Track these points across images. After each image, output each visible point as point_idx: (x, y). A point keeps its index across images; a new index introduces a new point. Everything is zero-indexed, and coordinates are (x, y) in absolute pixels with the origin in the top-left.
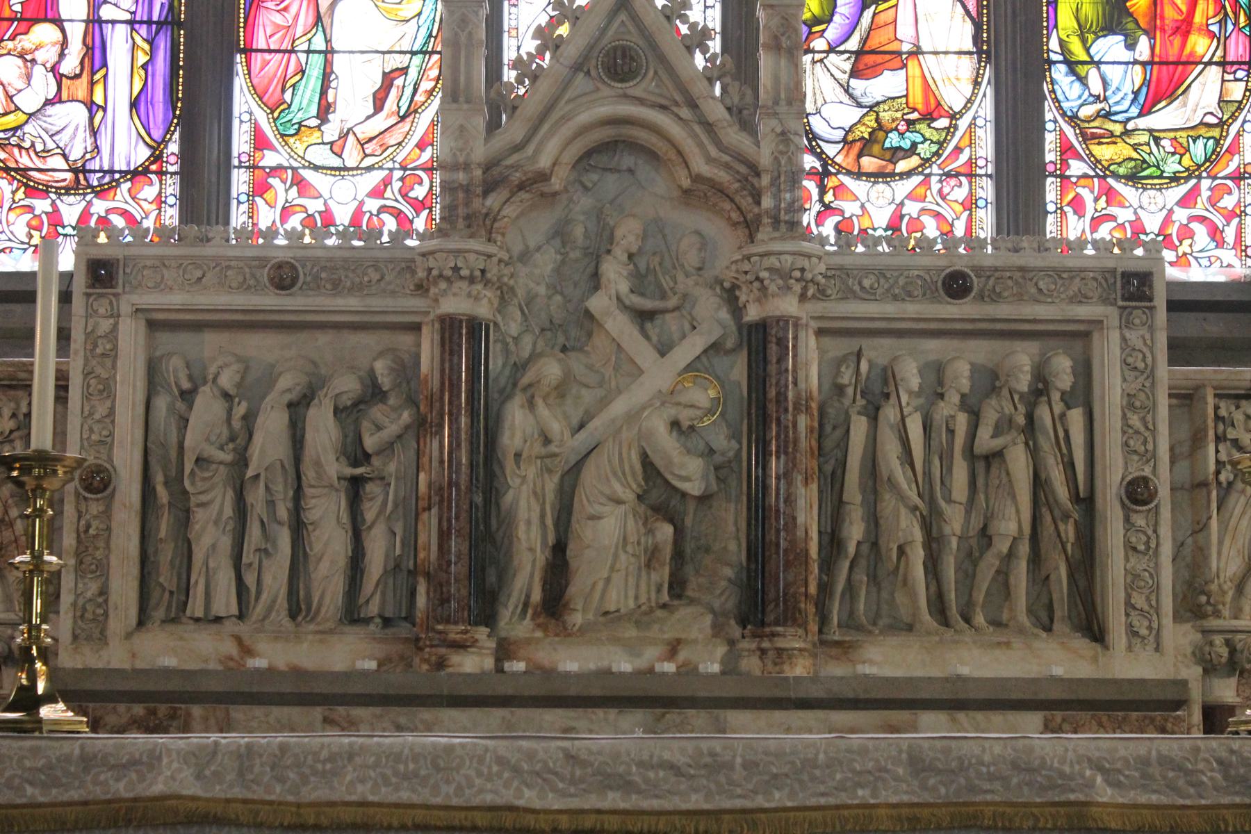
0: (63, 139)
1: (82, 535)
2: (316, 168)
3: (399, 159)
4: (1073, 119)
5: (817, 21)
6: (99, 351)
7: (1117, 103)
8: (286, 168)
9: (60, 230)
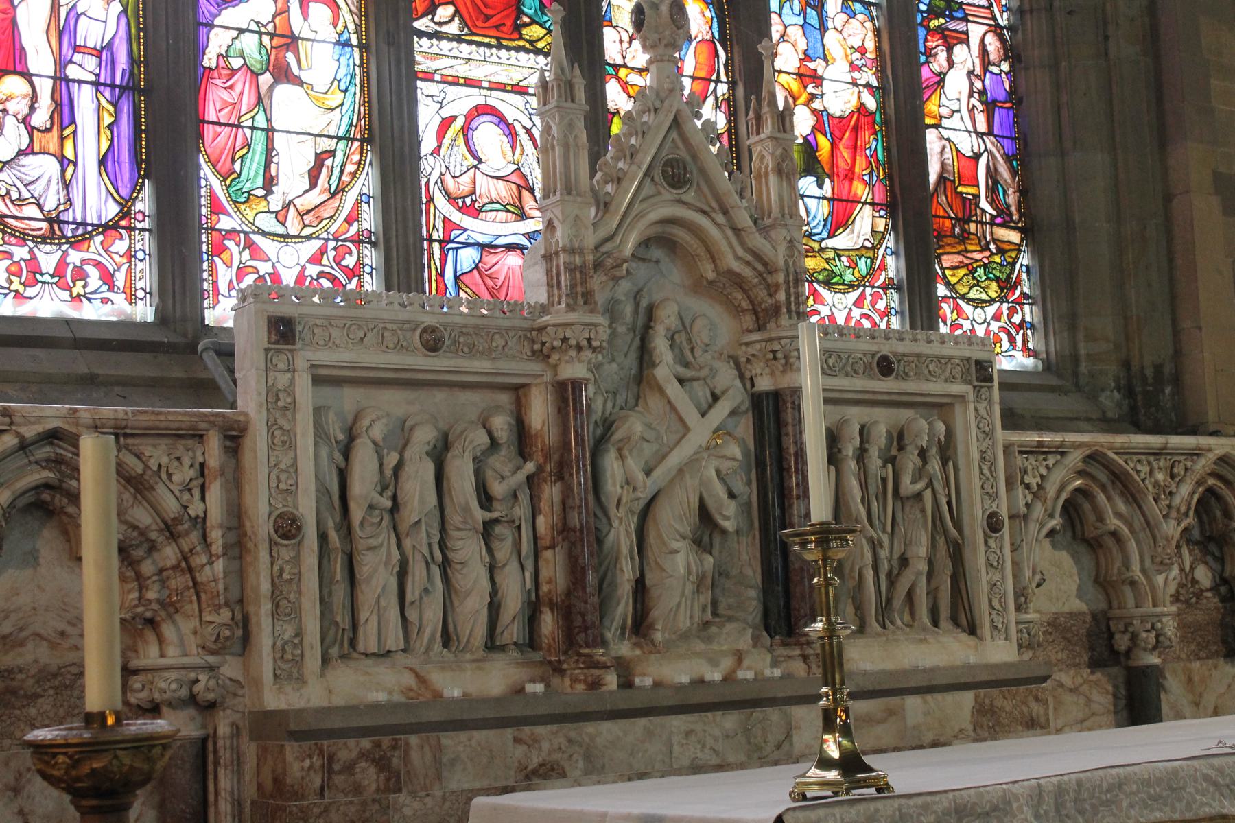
0: (38, 189)
1: (276, 580)
2: (265, 234)
3: (332, 230)
6: (280, 404)
7: (815, 227)
8: (239, 232)
9: (38, 276)
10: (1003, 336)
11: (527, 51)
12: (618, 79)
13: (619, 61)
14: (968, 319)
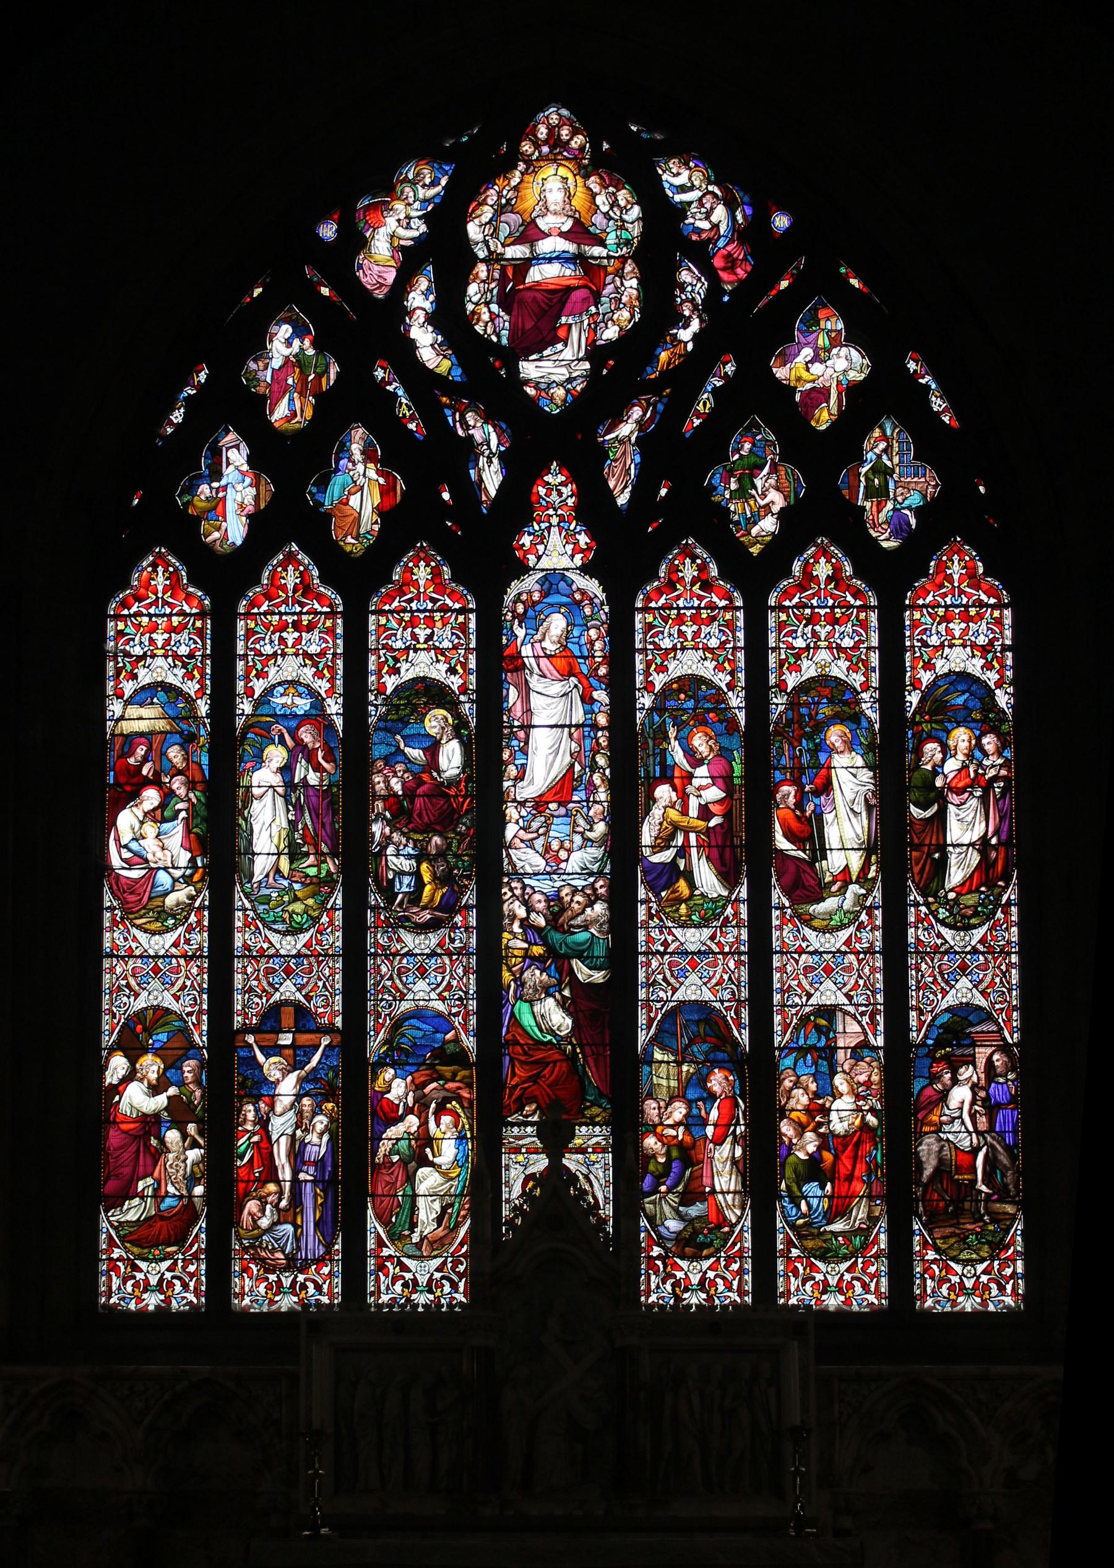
2: (409, 1257)
3: (451, 1251)
4: (792, 1226)
5: (661, 1176)
10: (993, 1285)
11: (587, 1125)
12: (655, 1134)
13: (656, 1120)
14: (957, 1274)
